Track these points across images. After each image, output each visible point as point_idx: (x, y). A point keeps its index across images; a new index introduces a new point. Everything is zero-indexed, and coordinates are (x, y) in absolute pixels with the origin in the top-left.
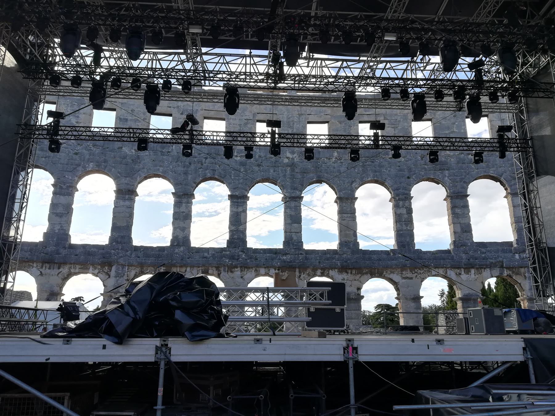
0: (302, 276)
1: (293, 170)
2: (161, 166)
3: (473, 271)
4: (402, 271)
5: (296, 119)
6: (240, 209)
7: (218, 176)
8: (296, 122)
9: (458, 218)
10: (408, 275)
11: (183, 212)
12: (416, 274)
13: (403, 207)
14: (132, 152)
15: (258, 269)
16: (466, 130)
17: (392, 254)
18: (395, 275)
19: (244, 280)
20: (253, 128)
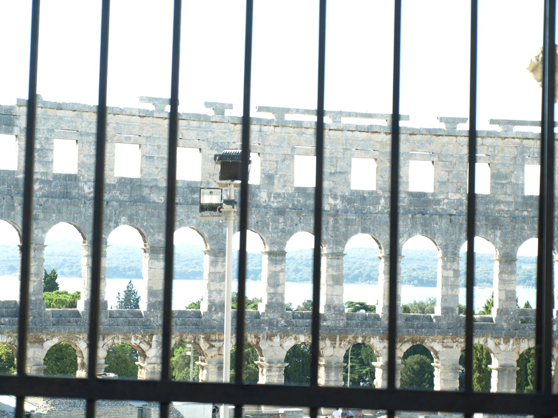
0: (343, 343)
1: (336, 221)
2: (194, 218)
3: (512, 341)
4: (443, 339)
5: (340, 155)
6: (279, 268)
7: (255, 229)
8: (339, 158)
9: (504, 284)
10: (449, 344)
11: (219, 273)
12: (456, 343)
13: (450, 269)
14: (161, 200)
15: (297, 336)
16: (524, 182)
17: (434, 320)
18: (436, 343)
19: (283, 348)
20: (291, 165)
